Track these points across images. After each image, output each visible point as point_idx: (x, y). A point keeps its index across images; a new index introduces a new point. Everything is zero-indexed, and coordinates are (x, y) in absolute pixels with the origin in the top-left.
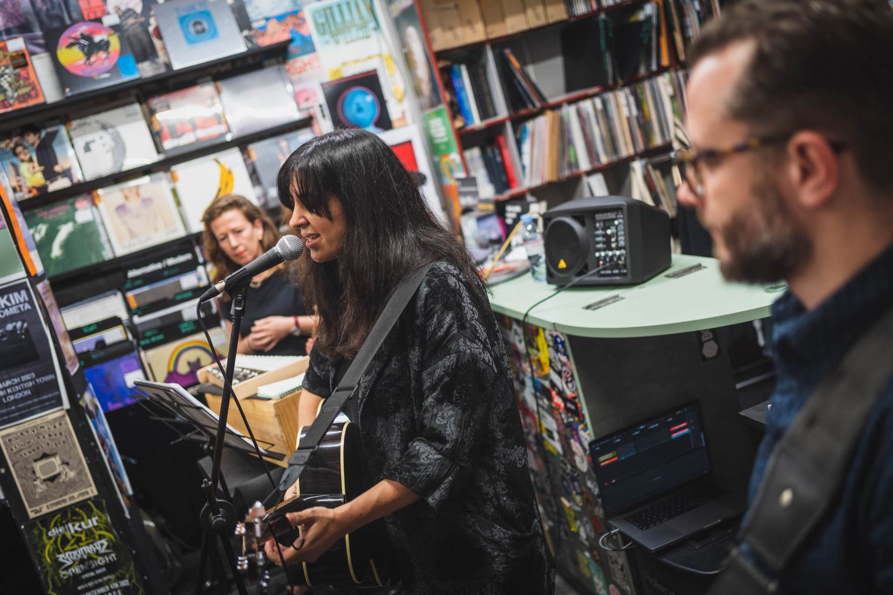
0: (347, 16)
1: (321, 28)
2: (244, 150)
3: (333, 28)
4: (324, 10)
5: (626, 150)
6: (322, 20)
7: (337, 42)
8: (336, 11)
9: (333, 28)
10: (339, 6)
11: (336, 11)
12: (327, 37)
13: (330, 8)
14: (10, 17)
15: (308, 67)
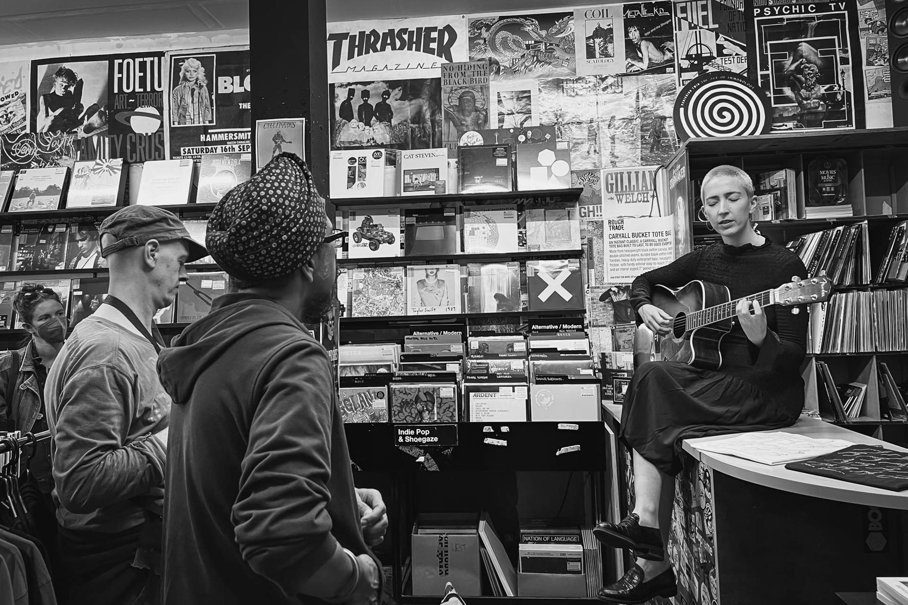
0: (633, 182)
1: (609, 186)
2: (523, 265)
3: (619, 190)
4: (616, 174)
5: (866, 347)
6: (614, 182)
7: (620, 200)
8: (625, 176)
9: (619, 190)
10: (629, 173)
11: (625, 176)
12: (613, 195)
13: (622, 174)
14: (394, 137)
15: (591, 214)
